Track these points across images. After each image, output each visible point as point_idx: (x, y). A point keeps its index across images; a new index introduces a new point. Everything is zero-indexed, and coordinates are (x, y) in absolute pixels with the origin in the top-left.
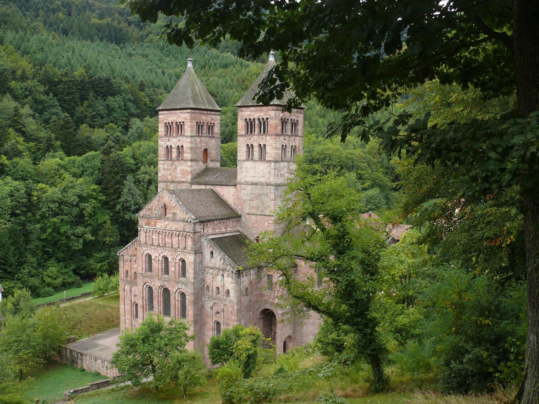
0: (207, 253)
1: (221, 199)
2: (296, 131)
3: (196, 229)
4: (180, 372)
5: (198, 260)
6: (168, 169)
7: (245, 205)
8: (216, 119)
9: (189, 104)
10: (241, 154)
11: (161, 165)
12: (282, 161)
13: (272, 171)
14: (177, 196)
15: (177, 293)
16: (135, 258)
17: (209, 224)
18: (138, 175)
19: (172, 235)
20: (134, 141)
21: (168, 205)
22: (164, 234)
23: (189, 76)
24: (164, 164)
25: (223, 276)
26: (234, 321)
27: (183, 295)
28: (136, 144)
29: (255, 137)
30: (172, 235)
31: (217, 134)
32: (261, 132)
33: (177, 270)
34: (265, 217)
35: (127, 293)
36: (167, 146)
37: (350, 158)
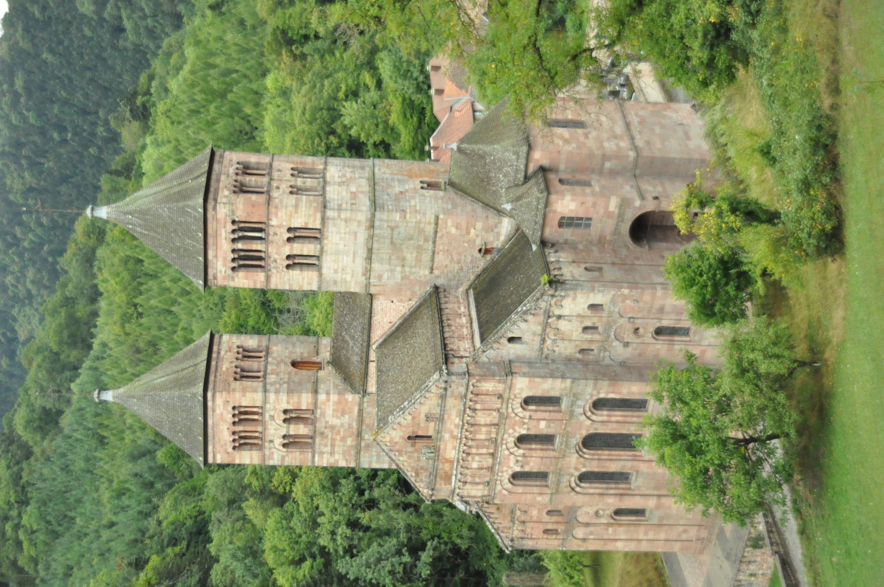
0: (512, 351)
1: (398, 329)
2: (261, 166)
3: (461, 371)
4: (763, 369)
5: (526, 370)
6: (333, 445)
7: (412, 277)
8: (229, 342)
9: (194, 395)
10: (306, 281)
11: (324, 460)
12: (323, 195)
13: (343, 215)
14: (391, 412)
15: (594, 417)
16: (518, 513)
17: (450, 346)
18: (336, 551)
19: (472, 425)
20: (263, 564)
21: (410, 432)
22: (470, 443)
23: (133, 397)
24: (322, 453)
25: (559, 317)
26: (654, 296)
27: (598, 404)
28: (270, 558)
29: (272, 250)
30: (472, 425)
31: (260, 341)
32: (260, 238)
33: (546, 415)
34: (439, 235)
35: (591, 533)
36: (284, 445)
37: (313, 114)
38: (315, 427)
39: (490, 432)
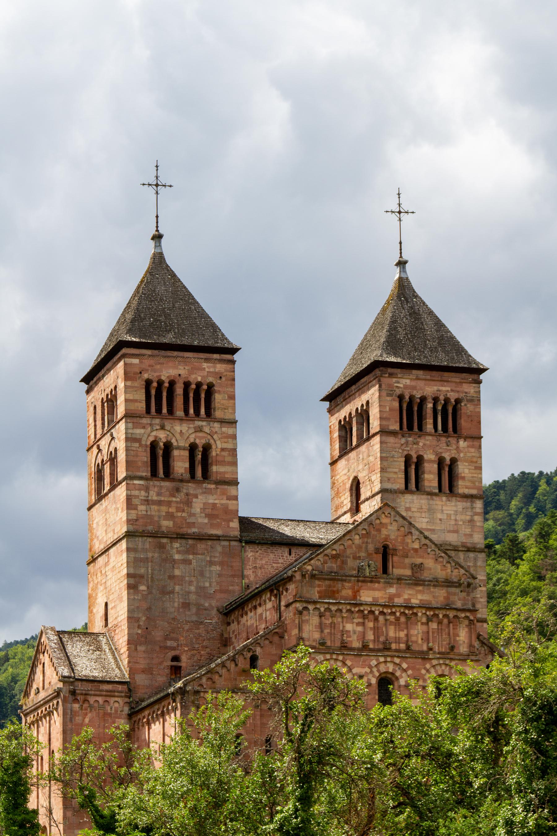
6: (159, 503)
24: (147, 489)
29: (428, 440)
38: (188, 482)
39: (398, 640)
